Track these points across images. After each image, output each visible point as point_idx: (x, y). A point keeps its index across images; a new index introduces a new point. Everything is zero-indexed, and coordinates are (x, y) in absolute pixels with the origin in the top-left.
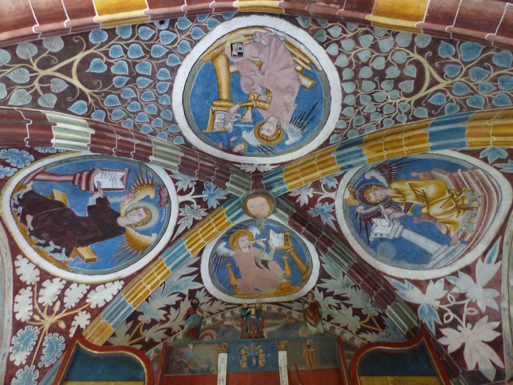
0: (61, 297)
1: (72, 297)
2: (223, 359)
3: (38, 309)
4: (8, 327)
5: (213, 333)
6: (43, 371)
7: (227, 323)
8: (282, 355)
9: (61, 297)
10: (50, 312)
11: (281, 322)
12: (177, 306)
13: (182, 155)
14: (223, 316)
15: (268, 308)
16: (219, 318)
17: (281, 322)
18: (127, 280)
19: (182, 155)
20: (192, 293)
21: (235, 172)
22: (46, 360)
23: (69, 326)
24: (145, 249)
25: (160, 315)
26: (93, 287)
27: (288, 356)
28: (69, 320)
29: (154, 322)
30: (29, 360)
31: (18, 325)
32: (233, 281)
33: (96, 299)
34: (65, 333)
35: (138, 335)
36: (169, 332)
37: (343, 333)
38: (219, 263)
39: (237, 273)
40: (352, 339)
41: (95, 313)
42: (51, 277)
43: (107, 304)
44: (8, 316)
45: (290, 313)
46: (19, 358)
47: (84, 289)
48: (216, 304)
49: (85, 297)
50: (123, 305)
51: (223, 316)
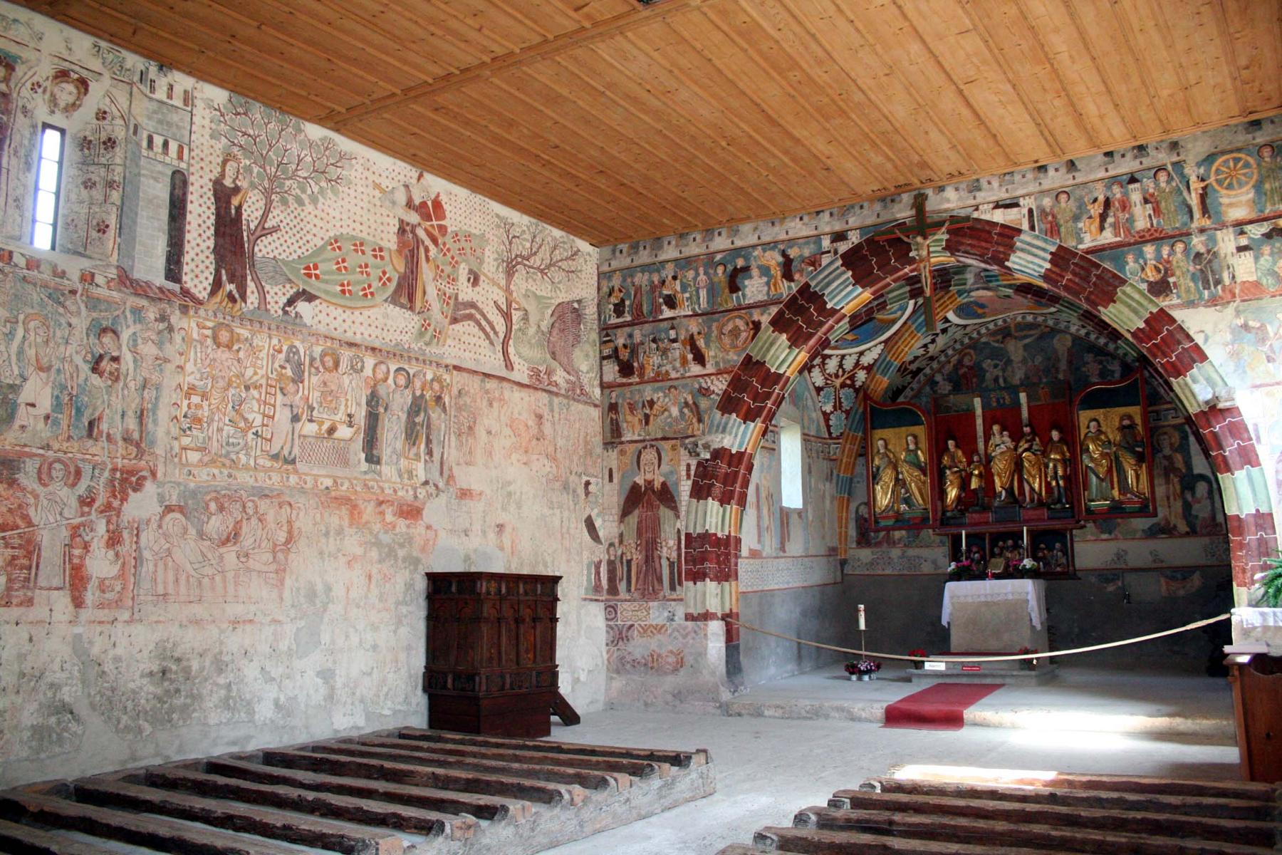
0: (841, 366)
1: (849, 364)
2: (977, 402)
3: (827, 377)
4: (814, 393)
5: (972, 352)
6: (847, 412)
7: (984, 340)
8: (1023, 397)
9: (841, 366)
10: (837, 376)
11: (1036, 332)
12: (933, 341)
13: (908, 288)
14: (979, 333)
15: (1024, 318)
16: (975, 335)
17: (1036, 332)
18: (886, 342)
19: (908, 288)
20: (944, 331)
21: (956, 273)
22: (846, 405)
23: (853, 382)
24: (894, 322)
25: (922, 351)
26: (861, 353)
27: (1029, 397)
28: (852, 378)
29: (916, 358)
30: (835, 407)
31: (819, 390)
32: (980, 311)
33: (866, 360)
34: (852, 386)
35: (906, 369)
36: (932, 359)
37: (1097, 338)
38: (962, 311)
39: (982, 306)
40: (1106, 344)
41: (869, 369)
42: (830, 356)
43: (876, 360)
44: (811, 387)
45: (1045, 321)
46: (828, 408)
47: (855, 357)
48: (968, 329)
49: (858, 361)
50: (889, 364)
51: (979, 333)
